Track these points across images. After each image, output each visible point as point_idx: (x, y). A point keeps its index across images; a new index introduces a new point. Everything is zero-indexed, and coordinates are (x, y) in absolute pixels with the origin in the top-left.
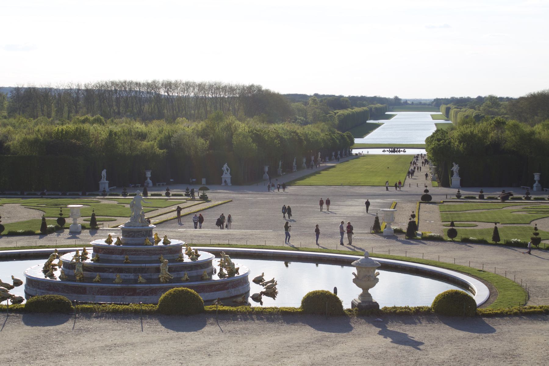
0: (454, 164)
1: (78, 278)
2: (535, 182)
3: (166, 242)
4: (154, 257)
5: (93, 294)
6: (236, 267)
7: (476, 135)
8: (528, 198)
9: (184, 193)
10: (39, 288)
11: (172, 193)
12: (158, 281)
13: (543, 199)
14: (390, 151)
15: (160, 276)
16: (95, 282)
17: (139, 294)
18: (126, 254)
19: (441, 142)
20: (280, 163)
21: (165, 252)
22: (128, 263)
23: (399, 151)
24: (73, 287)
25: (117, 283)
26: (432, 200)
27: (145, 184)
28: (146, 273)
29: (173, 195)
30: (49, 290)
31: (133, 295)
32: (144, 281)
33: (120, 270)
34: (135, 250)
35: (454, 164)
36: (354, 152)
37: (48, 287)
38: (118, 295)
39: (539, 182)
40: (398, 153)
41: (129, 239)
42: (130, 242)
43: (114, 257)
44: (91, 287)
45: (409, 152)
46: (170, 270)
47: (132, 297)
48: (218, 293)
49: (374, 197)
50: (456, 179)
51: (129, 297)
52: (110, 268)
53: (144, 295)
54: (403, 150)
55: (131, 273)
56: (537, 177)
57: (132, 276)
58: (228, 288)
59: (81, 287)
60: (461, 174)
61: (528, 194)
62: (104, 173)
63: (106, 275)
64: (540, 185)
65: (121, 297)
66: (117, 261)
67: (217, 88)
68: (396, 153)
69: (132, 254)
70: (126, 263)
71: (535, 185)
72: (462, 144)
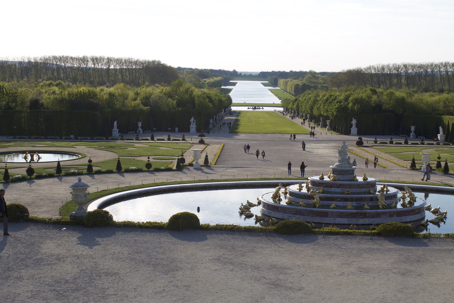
0: (353, 119)
1: (317, 205)
2: (411, 132)
3: (365, 179)
4: (363, 190)
5: (334, 217)
6: (415, 196)
7: (365, 99)
8: (423, 144)
9: (181, 139)
10: (285, 213)
11: (172, 138)
12: (377, 207)
13: (433, 144)
14: (253, 108)
16: (332, 208)
17: (368, 217)
18: (343, 188)
19: (342, 103)
22: (349, 194)
23: (259, 108)
25: (350, 209)
26: (364, 145)
27: (138, 132)
29: (173, 140)
30: (295, 214)
31: (364, 218)
32: (368, 207)
33: (346, 200)
35: (353, 119)
36: (233, 108)
37: (294, 212)
38: (353, 218)
39: (414, 132)
40: (259, 110)
41: (341, 176)
42: (341, 179)
43: (333, 190)
44: (333, 212)
45: (266, 109)
47: (364, 219)
48: (417, 215)
49: (316, 142)
50: (354, 130)
51: (361, 219)
52: (338, 198)
53: (372, 218)
54: (261, 107)
56: (413, 128)
57: (354, 204)
58: (420, 212)
59: (324, 212)
60: (357, 126)
61: (423, 140)
62: (115, 123)
66: (335, 193)
67: (130, 62)
68: (257, 110)
70: (347, 194)
71: (411, 134)
72: (356, 105)
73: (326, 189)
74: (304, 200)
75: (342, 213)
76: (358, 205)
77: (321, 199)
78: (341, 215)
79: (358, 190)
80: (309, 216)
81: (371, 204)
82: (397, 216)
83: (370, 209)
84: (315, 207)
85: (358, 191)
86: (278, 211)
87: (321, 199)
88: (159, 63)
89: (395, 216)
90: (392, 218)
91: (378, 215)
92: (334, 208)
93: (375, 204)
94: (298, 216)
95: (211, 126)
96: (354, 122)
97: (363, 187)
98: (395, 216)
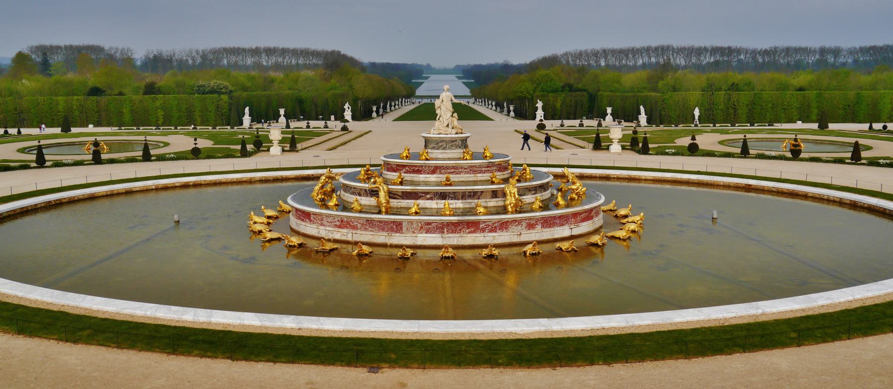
5: (413, 232)
10: (322, 225)
12: (504, 210)
15: (508, 202)
17: (483, 230)
22: (450, 185)
24: (380, 222)
30: (340, 227)
31: (474, 232)
34: (453, 167)
37: (338, 223)
42: (440, 156)
43: (422, 177)
44: (411, 222)
46: (522, 192)
47: (474, 235)
51: (470, 235)
52: (428, 193)
53: (491, 231)
55: (458, 199)
56: (609, 110)
57: (459, 204)
59: (394, 222)
60: (544, 109)
62: (247, 110)
63: (423, 203)
65: (457, 235)
66: (426, 184)
70: (446, 185)
73: (408, 177)
74: (363, 198)
75: (429, 224)
76: (468, 206)
77: (392, 195)
78: (428, 227)
79: (470, 177)
80: (366, 229)
81: (493, 203)
82: (543, 227)
83: (486, 214)
84: (380, 212)
85: (471, 179)
86: (310, 221)
87: (392, 195)
88: (339, 52)
89: (539, 227)
90: (532, 231)
92: (416, 213)
93: (501, 203)
94: (345, 230)
95: (374, 115)
96: (540, 105)
97: (481, 172)
98: (539, 227)
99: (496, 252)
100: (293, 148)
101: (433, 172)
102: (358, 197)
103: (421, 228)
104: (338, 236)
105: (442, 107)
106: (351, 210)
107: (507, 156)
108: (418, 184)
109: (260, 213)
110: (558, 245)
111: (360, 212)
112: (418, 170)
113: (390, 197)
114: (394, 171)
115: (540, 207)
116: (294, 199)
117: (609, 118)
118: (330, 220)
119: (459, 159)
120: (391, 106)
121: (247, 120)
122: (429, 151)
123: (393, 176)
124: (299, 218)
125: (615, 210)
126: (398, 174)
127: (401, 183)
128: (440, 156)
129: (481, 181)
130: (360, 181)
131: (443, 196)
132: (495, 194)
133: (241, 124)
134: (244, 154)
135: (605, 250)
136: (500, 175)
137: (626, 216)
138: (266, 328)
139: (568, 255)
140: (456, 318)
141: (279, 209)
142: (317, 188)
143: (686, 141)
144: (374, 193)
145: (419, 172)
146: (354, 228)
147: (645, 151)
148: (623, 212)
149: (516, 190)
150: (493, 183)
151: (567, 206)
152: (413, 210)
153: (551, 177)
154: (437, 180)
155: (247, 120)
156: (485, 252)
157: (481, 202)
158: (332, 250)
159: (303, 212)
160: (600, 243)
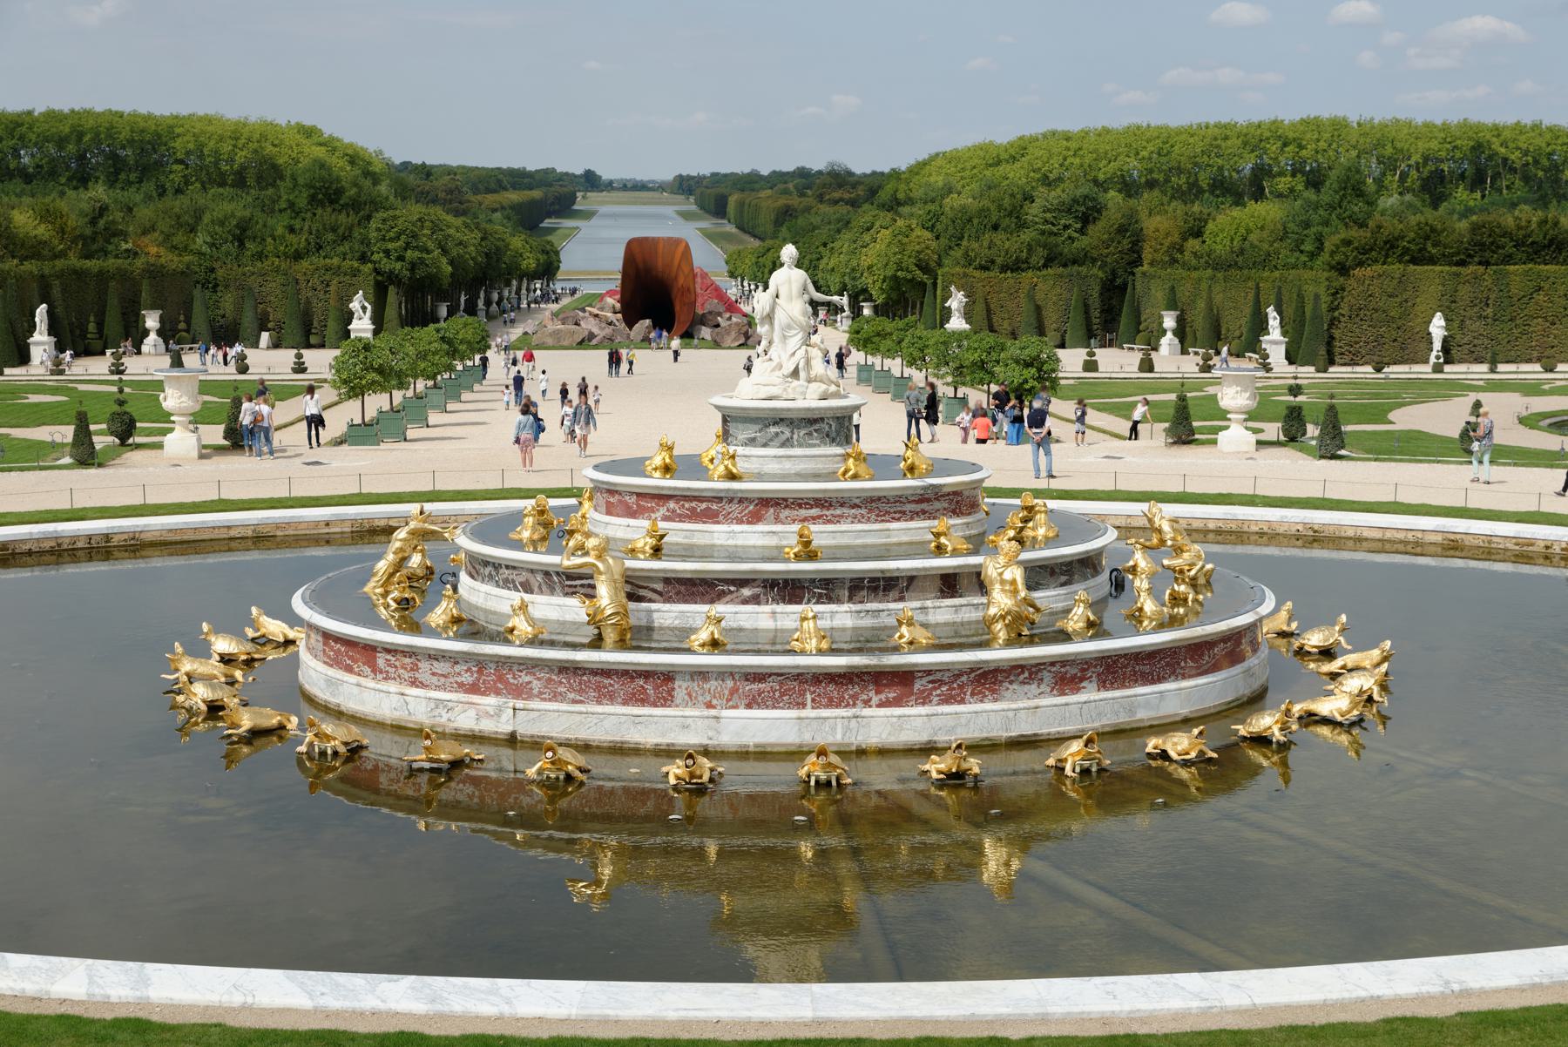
2: (1164, 332)
5: (710, 706)
10: (414, 683)
18: (777, 520)
20: (463, 299)
21: (937, 505)
22: (811, 556)
28: (902, 599)
30: (473, 689)
31: (897, 702)
35: (952, 288)
37: (467, 678)
42: (773, 467)
43: (721, 534)
44: (701, 674)
52: (742, 582)
55: (839, 601)
56: (1169, 322)
57: (842, 615)
62: (41, 312)
64: (1176, 341)
66: (733, 555)
69: (805, 520)
73: (678, 532)
75: (758, 676)
76: (867, 622)
77: (635, 588)
81: (944, 611)
82: (1103, 685)
84: (597, 643)
86: (375, 670)
88: (309, 132)
91: (988, 680)
92: (715, 645)
94: (490, 701)
96: (956, 301)
97: (902, 515)
99: (974, 765)
100: (239, 439)
101: (755, 518)
102: (527, 597)
103: (734, 691)
104: (466, 721)
105: (780, 317)
106: (505, 636)
107: (975, 467)
108: (706, 553)
109: (200, 649)
110: (1152, 744)
111: (533, 642)
112: (705, 507)
113: (632, 597)
114: (633, 514)
115: (1090, 624)
116: (315, 601)
117: (1168, 342)
118: (440, 667)
119: (831, 476)
120: (488, 303)
121: (41, 342)
122: (740, 450)
123: (634, 530)
124: (335, 662)
125: (1291, 634)
126: (645, 523)
127: (657, 551)
128: (769, 466)
129: (901, 543)
130: (518, 545)
131: (789, 589)
132: (949, 584)
133: (23, 358)
134: (85, 456)
135: (1293, 755)
136: (955, 527)
137: (1327, 653)
138: (328, 1014)
139: (1184, 774)
140: (900, 976)
141: (250, 633)
142: (382, 566)
143: (1445, 418)
144: (577, 582)
145: (710, 516)
146: (519, 692)
147: (1333, 446)
148: (1315, 639)
149: (1017, 574)
150: (940, 550)
151: (1173, 622)
152: (704, 636)
153: (1112, 535)
154: (772, 541)
155: (41, 342)
156: (936, 767)
157: (909, 606)
158: (457, 764)
159: (349, 643)
160: (1278, 735)
